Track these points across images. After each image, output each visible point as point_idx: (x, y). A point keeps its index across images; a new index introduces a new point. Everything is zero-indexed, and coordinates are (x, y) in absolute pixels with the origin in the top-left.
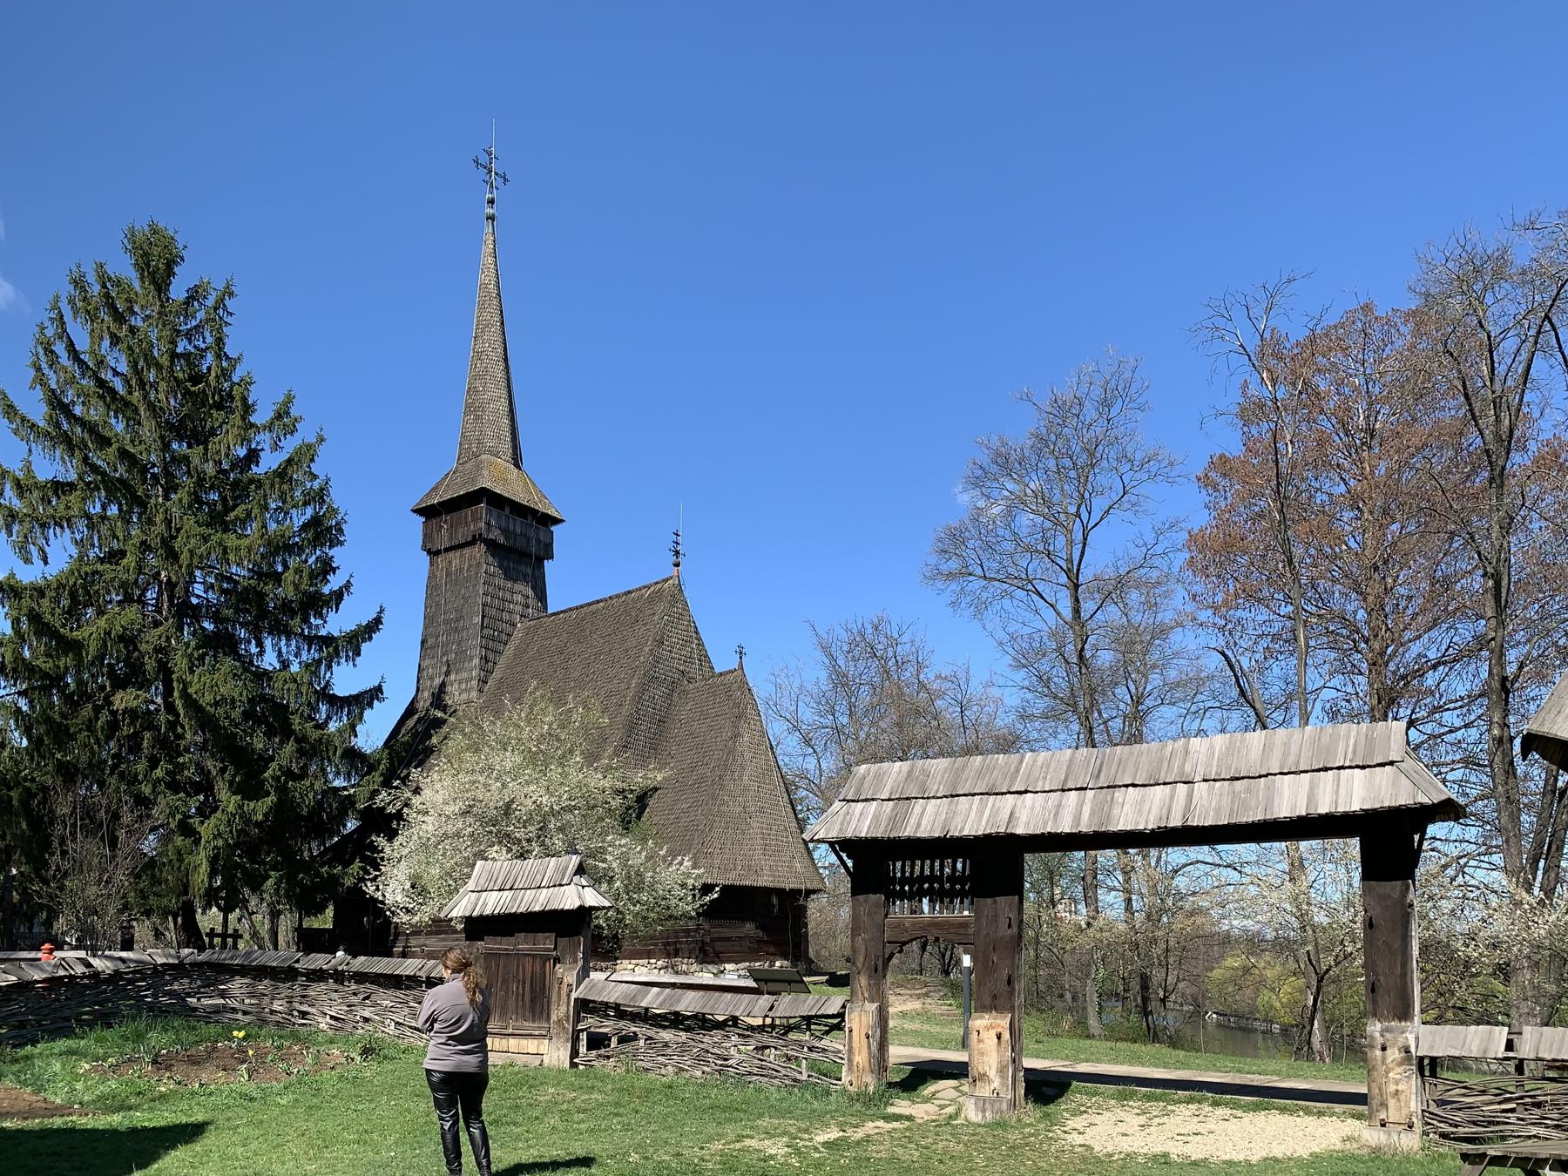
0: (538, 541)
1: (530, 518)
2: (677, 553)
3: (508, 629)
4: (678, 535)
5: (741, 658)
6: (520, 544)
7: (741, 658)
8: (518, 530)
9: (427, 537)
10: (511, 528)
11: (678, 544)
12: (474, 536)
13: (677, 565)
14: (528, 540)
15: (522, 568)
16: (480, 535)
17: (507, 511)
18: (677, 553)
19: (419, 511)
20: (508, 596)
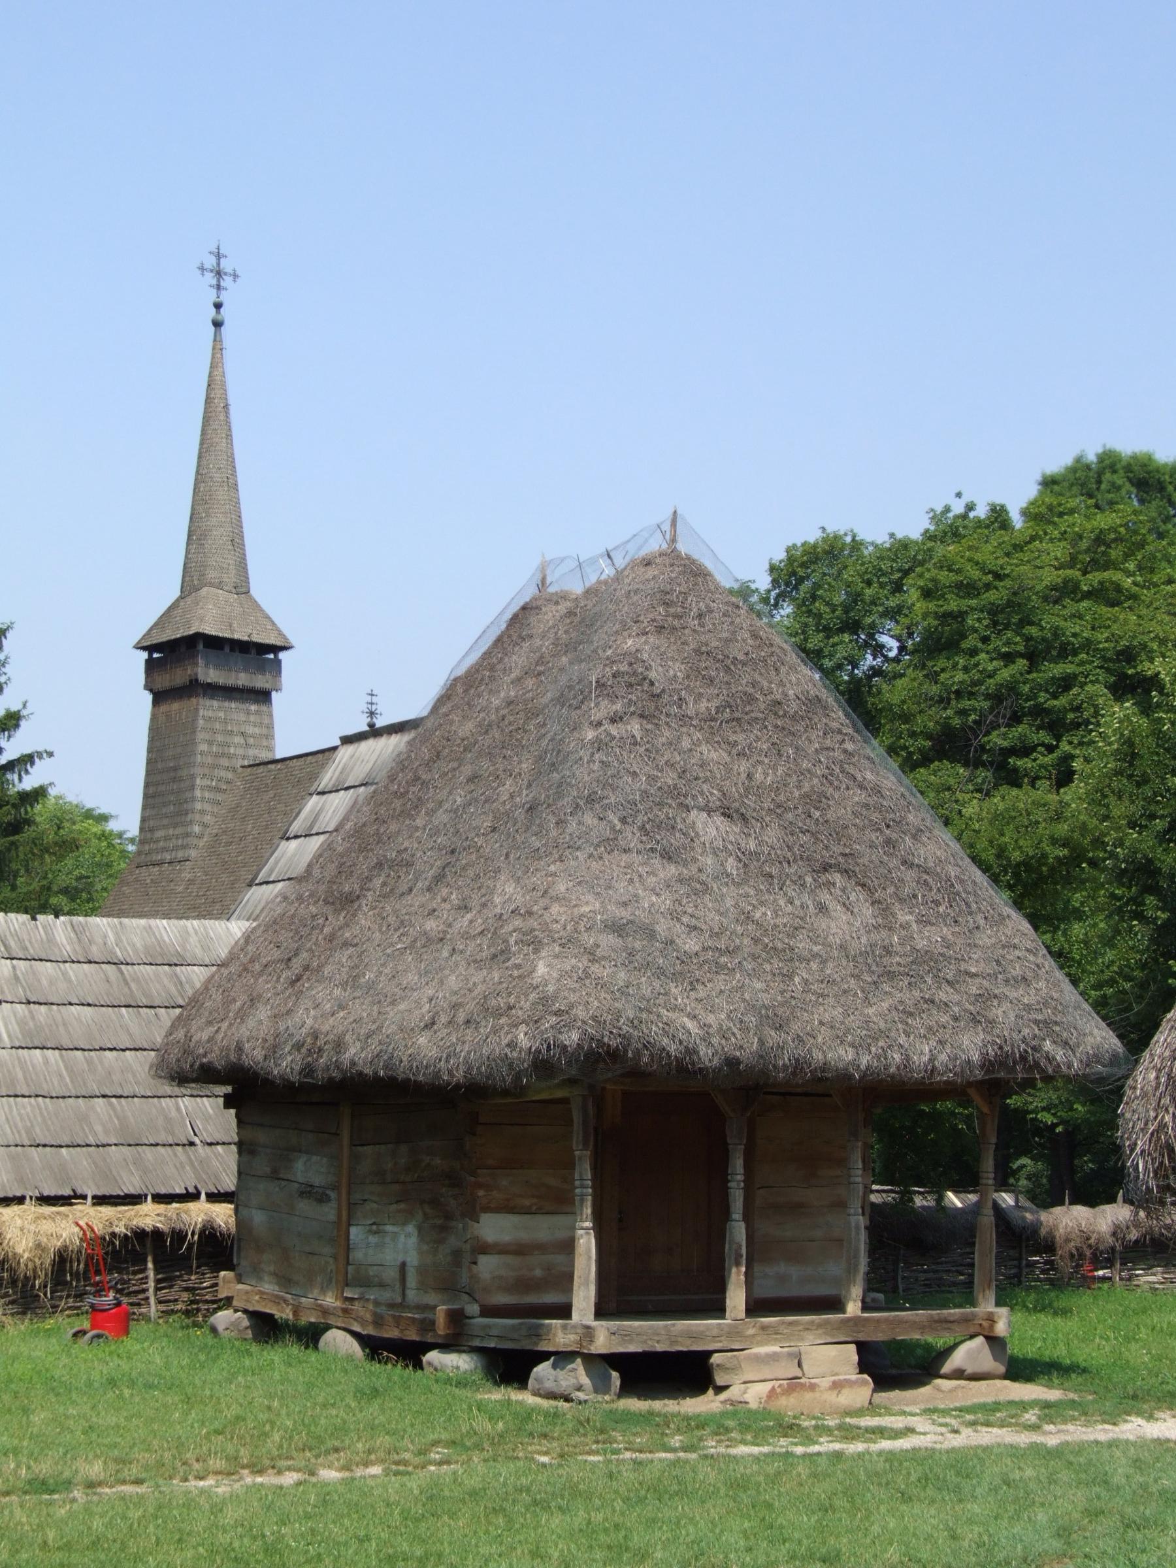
11: (372, 704)
17: (227, 649)
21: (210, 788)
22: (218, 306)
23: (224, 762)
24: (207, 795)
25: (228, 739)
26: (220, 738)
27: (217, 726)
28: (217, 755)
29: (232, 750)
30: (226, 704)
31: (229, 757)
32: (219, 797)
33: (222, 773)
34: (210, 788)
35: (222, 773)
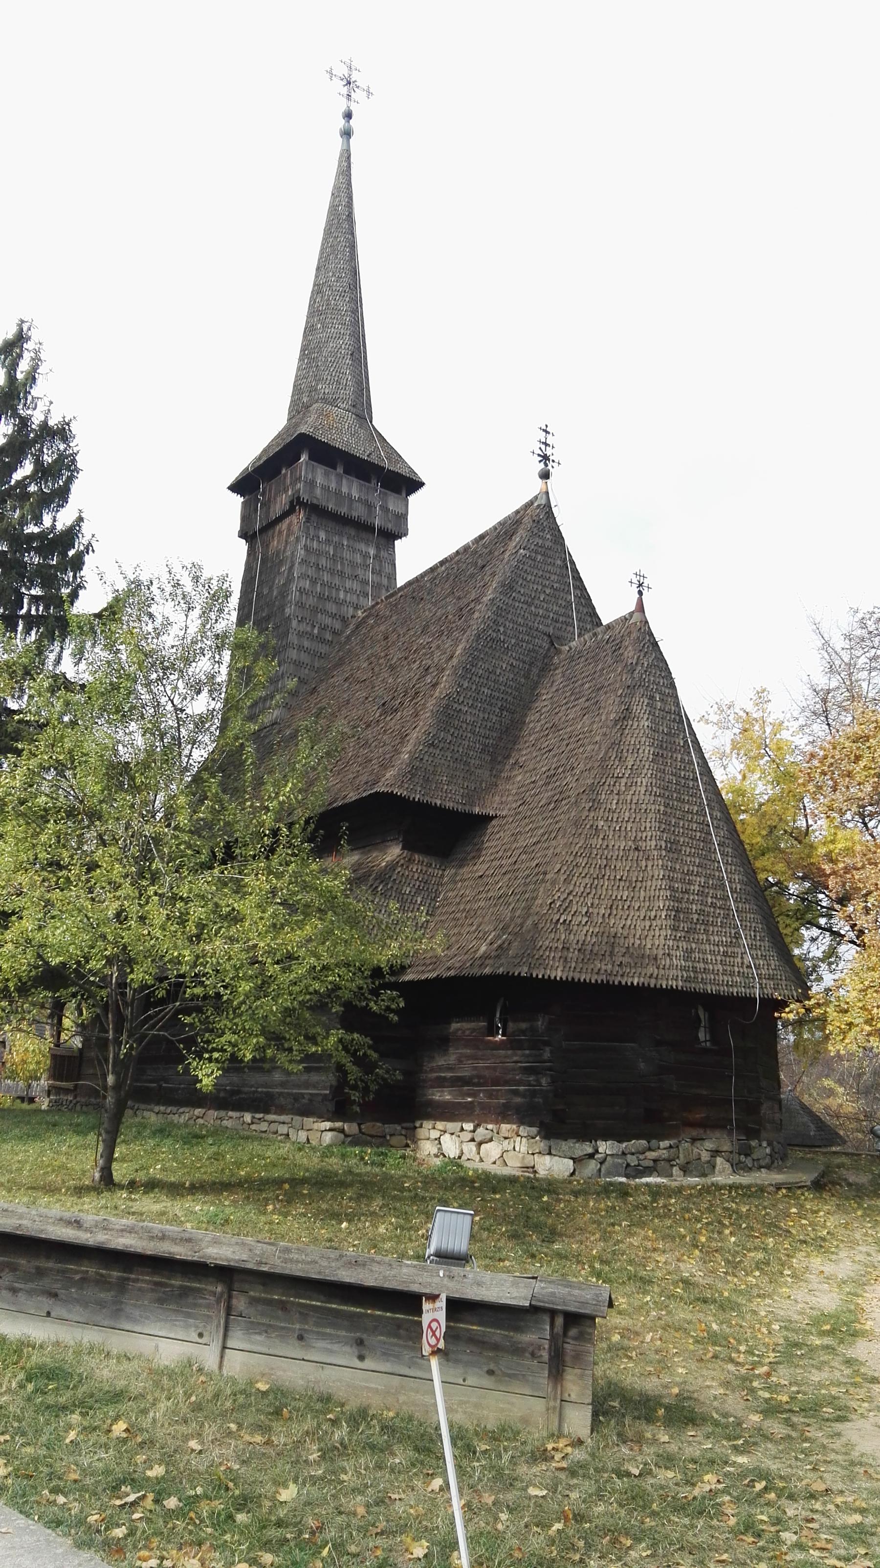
0: (385, 509)
1: (374, 481)
2: (545, 458)
3: (337, 625)
4: (547, 432)
5: (640, 593)
6: (358, 512)
7: (640, 593)
8: (355, 494)
9: (246, 519)
10: (345, 489)
11: (546, 444)
12: (292, 502)
13: (545, 475)
14: (370, 507)
15: (362, 547)
16: (298, 498)
17: (340, 470)
18: (545, 458)
19: (236, 488)
20: (337, 581)
21: (310, 636)
22: (348, 115)
23: (331, 607)
24: (306, 644)
25: (337, 581)
26: (326, 577)
27: (323, 562)
28: (321, 597)
29: (342, 595)
30: (336, 539)
31: (339, 603)
32: (323, 649)
33: (328, 621)
34: (310, 636)
35: (328, 621)
